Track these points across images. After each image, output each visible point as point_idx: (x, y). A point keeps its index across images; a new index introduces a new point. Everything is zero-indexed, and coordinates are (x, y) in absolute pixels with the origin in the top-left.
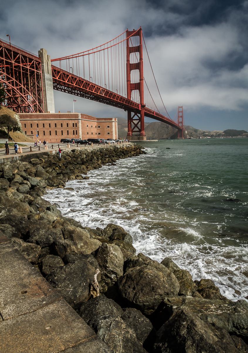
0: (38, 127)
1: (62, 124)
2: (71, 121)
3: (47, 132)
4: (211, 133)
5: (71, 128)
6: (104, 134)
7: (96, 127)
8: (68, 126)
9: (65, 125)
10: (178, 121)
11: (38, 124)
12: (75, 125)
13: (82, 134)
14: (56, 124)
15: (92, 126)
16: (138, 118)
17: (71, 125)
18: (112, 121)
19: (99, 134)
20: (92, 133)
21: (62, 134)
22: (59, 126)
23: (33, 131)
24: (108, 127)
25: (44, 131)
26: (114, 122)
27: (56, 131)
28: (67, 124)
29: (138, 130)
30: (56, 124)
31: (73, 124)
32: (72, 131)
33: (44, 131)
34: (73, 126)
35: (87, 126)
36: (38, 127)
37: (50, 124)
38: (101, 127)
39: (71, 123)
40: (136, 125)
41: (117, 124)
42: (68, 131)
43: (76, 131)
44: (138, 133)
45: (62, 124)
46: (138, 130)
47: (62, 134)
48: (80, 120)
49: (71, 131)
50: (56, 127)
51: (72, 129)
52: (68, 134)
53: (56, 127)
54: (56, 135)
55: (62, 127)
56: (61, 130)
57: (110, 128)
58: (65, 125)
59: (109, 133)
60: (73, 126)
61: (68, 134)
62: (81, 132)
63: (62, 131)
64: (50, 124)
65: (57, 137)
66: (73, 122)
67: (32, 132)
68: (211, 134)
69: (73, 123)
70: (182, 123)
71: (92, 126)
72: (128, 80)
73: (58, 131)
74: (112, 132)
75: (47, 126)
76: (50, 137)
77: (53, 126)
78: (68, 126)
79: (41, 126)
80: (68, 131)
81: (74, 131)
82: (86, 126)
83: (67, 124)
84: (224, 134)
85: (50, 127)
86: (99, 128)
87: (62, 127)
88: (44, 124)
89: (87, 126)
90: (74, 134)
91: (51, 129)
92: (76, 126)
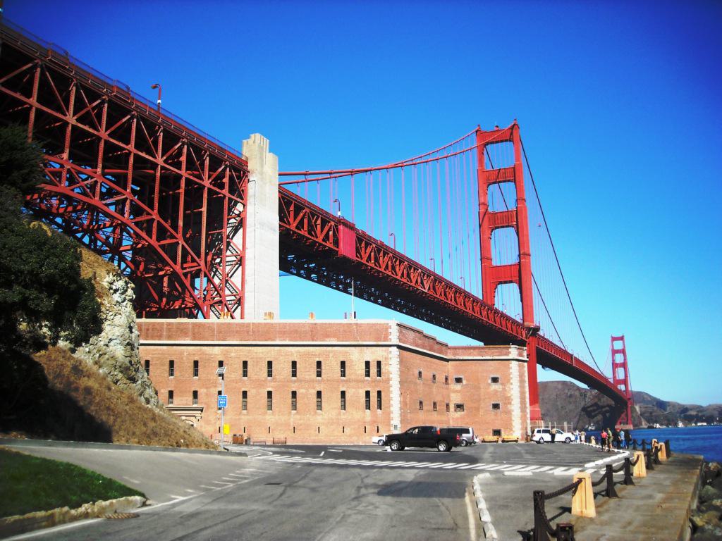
3: (257, 397)
5: (358, 381)
6: (478, 409)
8: (343, 375)
9: (331, 369)
12: (373, 370)
14: (294, 364)
17: (357, 369)
22: (307, 371)
24: (495, 380)
28: (343, 364)
30: (294, 364)
31: (367, 363)
34: (368, 374)
37: (270, 363)
38: (464, 382)
39: (357, 359)
41: (526, 369)
42: (343, 394)
43: (379, 393)
45: (319, 364)
49: (356, 394)
50: (294, 374)
51: (360, 384)
53: (294, 374)
55: (319, 374)
57: (502, 384)
58: (331, 369)
59: (496, 406)
60: (368, 374)
64: (270, 363)
65: (298, 417)
66: (372, 355)
70: (625, 382)
73: (300, 392)
74: (508, 400)
76: (270, 418)
77: (282, 369)
78: (343, 375)
80: (343, 394)
81: (368, 393)
83: (343, 364)
85: (270, 374)
86: (458, 387)
88: (245, 363)
91: (272, 384)
92: (379, 374)
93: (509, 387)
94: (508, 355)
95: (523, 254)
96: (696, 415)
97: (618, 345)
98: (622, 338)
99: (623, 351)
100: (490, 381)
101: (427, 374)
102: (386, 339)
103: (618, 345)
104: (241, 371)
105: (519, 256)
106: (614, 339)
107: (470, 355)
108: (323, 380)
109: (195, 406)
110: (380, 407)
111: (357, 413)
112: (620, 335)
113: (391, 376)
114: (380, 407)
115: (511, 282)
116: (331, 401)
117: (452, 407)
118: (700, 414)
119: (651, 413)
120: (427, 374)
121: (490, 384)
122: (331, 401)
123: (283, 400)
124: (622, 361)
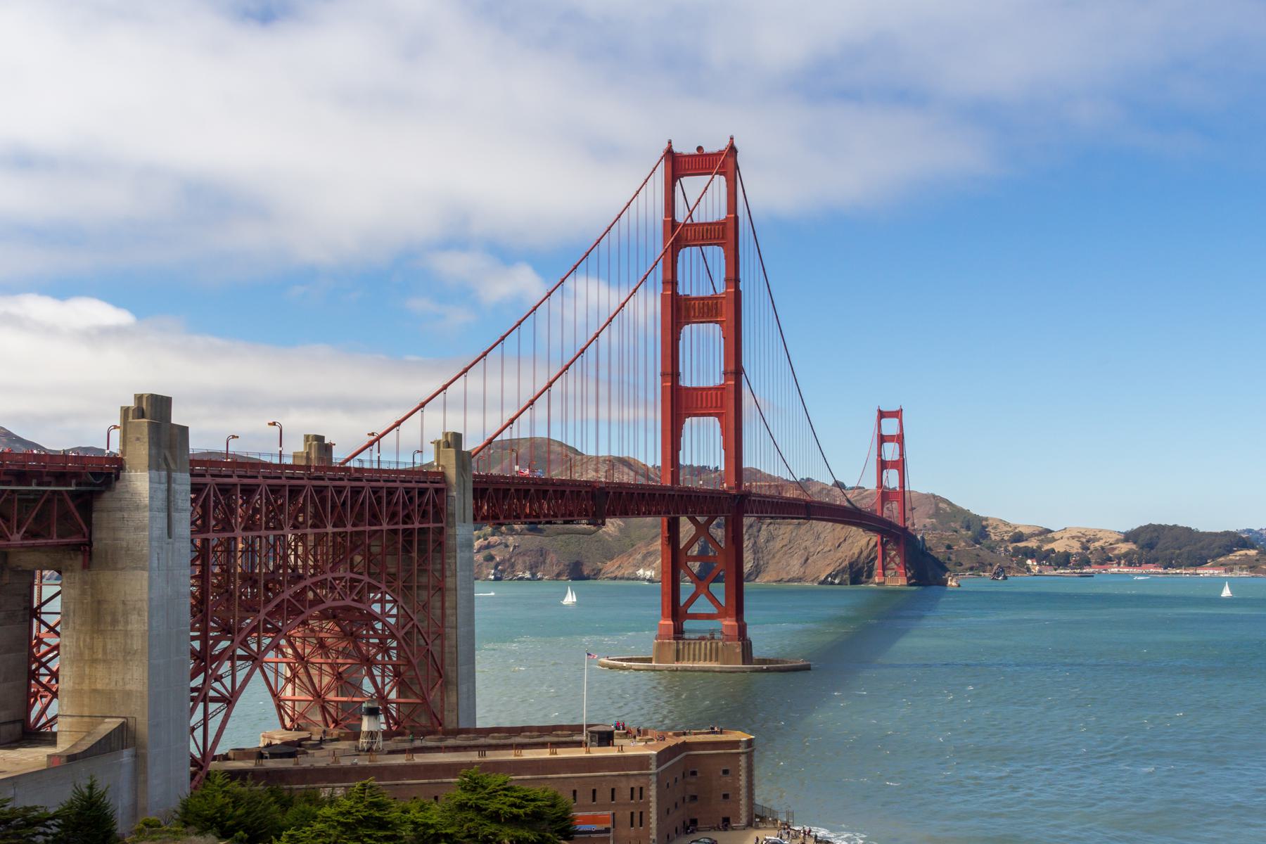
1: (594, 791)
2: (623, 779)
4: (1054, 540)
8: (613, 799)
9: (604, 795)
12: (637, 794)
18: (740, 751)
19: (694, 798)
20: (676, 804)
24: (726, 772)
28: (613, 790)
29: (712, 609)
31: (632, 789)
32: (628, 814)
38: (699, 775)
39: (624, 789)
43: (641, 813)
45: (594, 791)
46: (712, 609)
55: (594, 800)
58: (604, 795)
59: (726, 796)
60: (632, 798)
68: (1059, 547)
69: (633, 786)
72: (672, 370)
74: (738, 790)
78: (613, 799)
81: (632, 813)
82: (666, 784)
83: (613, 790)
84: (1124, 548)
86: (693, 779)
87: (594, 800)
90: (632, 826)
92: (641, 798)
93: (738, 779)
95: (735, 371)
96: (1039, 548)
97: (890, 427)
98: (897, 414)
99: (900, 439)
100: (721, 773)
103: (890, 427)
105: (725, 373)
106: (882, 415)
110: (641, 826)
112: (896, 408)
113: (651, 799)
115: (710, 415)
117: (687, 800)
118: (1046, 547)
119: (949, 547)
121: (721, 776)
124: (896, 457)
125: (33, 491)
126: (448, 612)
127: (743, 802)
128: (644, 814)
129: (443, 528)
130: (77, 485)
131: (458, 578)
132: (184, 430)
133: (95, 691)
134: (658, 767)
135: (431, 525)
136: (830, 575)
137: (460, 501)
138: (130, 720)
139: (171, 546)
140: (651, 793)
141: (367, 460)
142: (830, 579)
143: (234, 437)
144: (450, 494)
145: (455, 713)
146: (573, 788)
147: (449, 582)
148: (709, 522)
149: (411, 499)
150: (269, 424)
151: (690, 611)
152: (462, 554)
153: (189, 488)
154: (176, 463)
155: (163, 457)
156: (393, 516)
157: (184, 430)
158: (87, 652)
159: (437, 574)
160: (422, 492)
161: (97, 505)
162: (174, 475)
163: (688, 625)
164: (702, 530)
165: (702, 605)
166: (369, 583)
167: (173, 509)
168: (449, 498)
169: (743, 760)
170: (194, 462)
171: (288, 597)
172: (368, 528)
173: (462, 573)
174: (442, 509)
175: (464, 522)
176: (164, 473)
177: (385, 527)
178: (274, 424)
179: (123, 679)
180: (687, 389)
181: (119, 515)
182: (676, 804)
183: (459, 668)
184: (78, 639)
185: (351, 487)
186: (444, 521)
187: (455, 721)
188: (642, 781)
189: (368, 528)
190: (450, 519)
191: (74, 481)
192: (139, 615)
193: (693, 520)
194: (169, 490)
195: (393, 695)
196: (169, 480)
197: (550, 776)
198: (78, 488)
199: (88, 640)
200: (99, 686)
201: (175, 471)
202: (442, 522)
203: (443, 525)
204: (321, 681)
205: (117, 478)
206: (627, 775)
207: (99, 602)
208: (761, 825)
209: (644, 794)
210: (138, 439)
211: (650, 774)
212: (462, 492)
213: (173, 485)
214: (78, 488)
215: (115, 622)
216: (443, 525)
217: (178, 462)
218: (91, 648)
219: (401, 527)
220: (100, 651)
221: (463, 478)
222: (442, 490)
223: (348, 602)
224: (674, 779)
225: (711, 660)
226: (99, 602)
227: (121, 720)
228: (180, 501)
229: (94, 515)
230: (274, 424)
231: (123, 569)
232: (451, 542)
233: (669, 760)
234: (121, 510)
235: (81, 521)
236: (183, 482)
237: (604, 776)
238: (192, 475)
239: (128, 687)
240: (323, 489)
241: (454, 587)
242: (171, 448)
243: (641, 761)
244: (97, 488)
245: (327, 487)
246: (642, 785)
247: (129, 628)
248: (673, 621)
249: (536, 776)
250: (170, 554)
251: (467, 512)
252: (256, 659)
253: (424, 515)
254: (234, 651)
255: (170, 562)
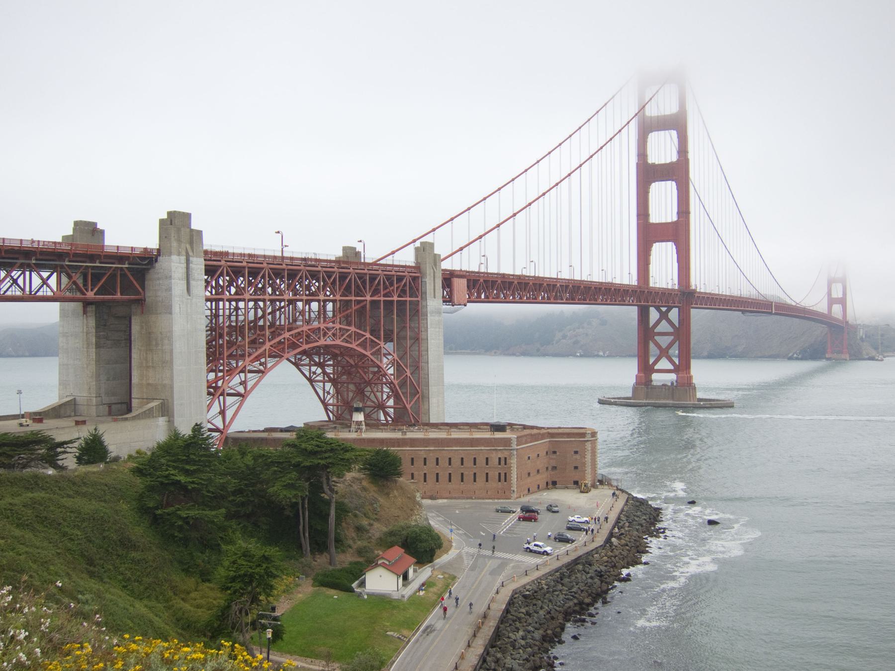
0: (425, 464)
1: (475, 459)
2: (494, 452)
3: (444, 477)
7: (547, 453)
8: (487, 464)
9: (481, 461)
10: (829, 293)
11: (425, 459)
12: (503, 462)
13: (517, 481)
14: (462, 459)
15: (538, 455)
16: (671, 330)
18: (586, 439)
19: (554, 468)
20: (538, 471)
21: (475, 481)
22: (469, 463)
23: (416, 473)
24: (576, 452)
25: (437, 474)
26: (590, 442)
27: (462, 474)
28: (487, 459)
29: (671, 367)
30: (462, 459)
31: (500, 459)
33: (437, 474)
35: (529, 458)
36: (425, 464)
37: (450, 459)
38: (558, 453)
40: (664, 353)
42: (487, 474)
43: (505, 474)
44: (673, 377)
45: (475, 459)
46: (671, 367)
47: (475, 481)
48: (514, 450)
49: (494, 474)
50: (462, 464)
52: (487, 481)
53: (462, 464)
54: (462, 481)
55: (475, 464)
56: (472, 471)
57: (580, 455)
58: (481, 461)
59: (576, 468)
60: (500, 464)
61: (487, 481)
62: (516, 476)
63: (475, 474)
64: (450, 459)
65: (464, 486)
67: (412, 474)
69: (500, 456)
70: (843, 301)
71: (538, 455)
73: (465, 473)
74: (584, 464)
75: (444, 463)
76: (450, 486)
77: (456, 462)
78: (487, 464)
79: (431, 463)
80: (487, 474)
81: (500, 474)
82: (527, 458)
83: (487, 459)
85: (450, 464)
86: (554, 456)
87: (475, 464)
88: (437, 459)
89: (529, 458)
92: (505, 464)
94: (584, 437)
100: (573, 453)
101: (533, 456)
102: (510, 446)
104: (435, 463)
105: (678, 213)
107: (562, 438)
108: (476, 468)
109: (412, 481)
110: (505, 481)
111: (493, 484)
114: (505, 481)
115: (669, 241)
116: (481, 478)
120: (533, 456)
122: (481, 478)
123: (456, 478)
125: (97, 267)
126: (424, 353)
127: (589, 470)
128: (507, 475)
129: (419, 301)
130: (129, 264)
131: (429, 332)
132: (200, 233)
133: (148, 384)
134: (517, 445)
135: (408, 299)
136: (795, 353)
137: (433, 287)
138: (166, 401)
139: (189, 301)
140: (512, 461)
141: (388, 261)
142: (795, 355)
143: (286, 246)
144: (423, 280)
145: (427, 415)
146: (461, 456)
147: (423, 335)
148: (670, 309)
149: (392, 284)
150: (276, 232)
151: (656, 367)
152: (432, 318)
153: (204, 267)
154: (193, 251)
155: (185, 248)
156: (376, 292)
157: (200, 233)
158: (144, 361)
159: (416, 330)
160: (400, 279)
161: (148, 277)
162: (191, 259)
163: (655, 376)
164: (664, 316)
165: (664, 364)
166: (355, 332)
167: (191, 279)
168: (423, 283)
169: (588, 446)
170: (206, 252)
171: (288, 336)
172: (353, 298)
173: (433, 329)
174: (417, 289)
175: (435, 297)
176: (183, 258)
177: (368, 298)
178: (278, 232)
179: (162, 377)
180: (653, 224)
181: (158, 282)
182: (538, 471)
183: (430, 388)
184: (140, 354)
185: (339, 273)
186: (420, 297)
187: (428, 419)
188: (506, 454)
189: (353, 298)
190: (424, 296)
191: (127, 262)
192: (169, 340)
193: (658, 308)
194: (188, 268)
195: (391, 402)
196: (188, 262)
197: (446, 448)
198: (130, 266)
199: (144, 355)
200: (150, 382)
201: (192, 256)
202: (418, 297)
203: (419, 299)
204: (348, 394)
205: (156, 261)
206: (496, 450)
207: (150, 333)
208: (600, 487)
209: (507, 462)
210: (166, 237)
211: (511, 450)
212: (432, 279)
213: (191, 265)
214: (130, 266)
215: (157, 345)
216: (419, 299)
217: (195, 250)
218: (146, 360)
219: (382, 299)
220: (151, 361)
221: (434, 270)
222: (418, 277)
223: (338, 342)
224: (536, 455)
225: (668, 399)
226: (150, 333)
227: (161, 401)
228: (196, 275)
229: (146, 283)
230: (278, 232)
231: (160, 313)
232: (424, 310)
233: (531, 442)
234: (159, 279)
235: (138, 286)
236: (198, 265)
237: (482, 450)
238: (205, 260)
239: (164, 382)
240: (316, 273)
241: (426, 337)
242: (191, 243)
243: (507, 442)
244: (144, 267)
245: (319, 272)
246: (506, 456)
247: (164, 348)
248: (644, 373)
249: (437, 448)
250: (189, 306)
251: (437, 291)
252: (264, 372)
253: (403, 293)
254: (245, 367)
255: (189, 311)
